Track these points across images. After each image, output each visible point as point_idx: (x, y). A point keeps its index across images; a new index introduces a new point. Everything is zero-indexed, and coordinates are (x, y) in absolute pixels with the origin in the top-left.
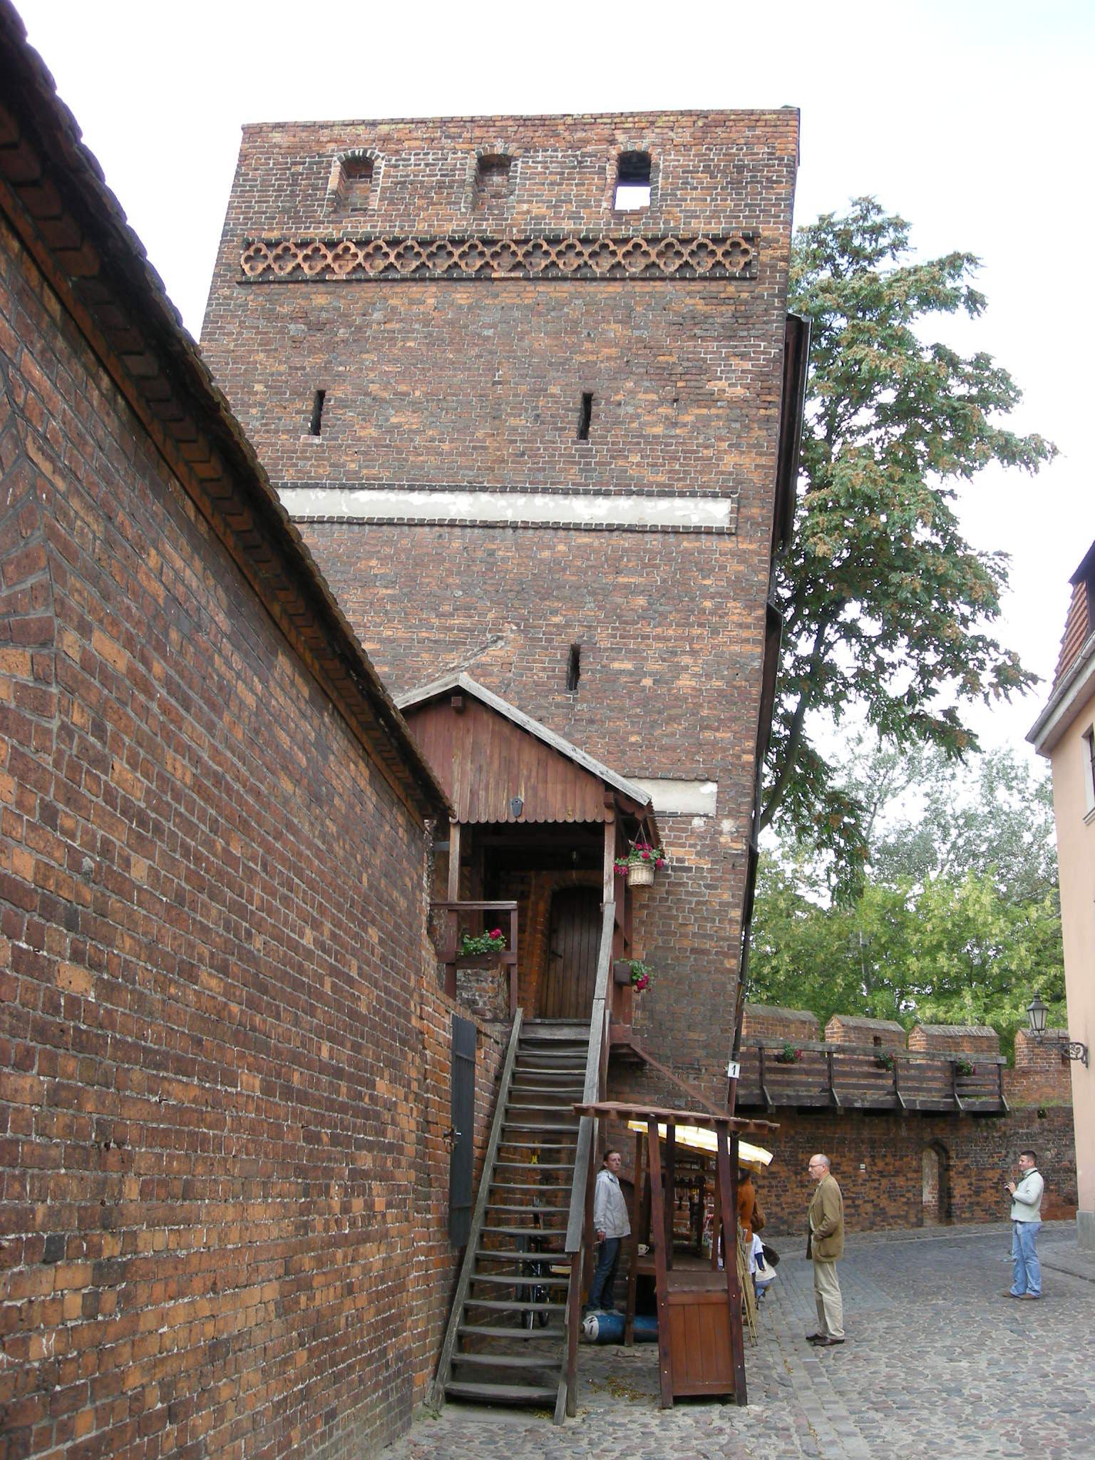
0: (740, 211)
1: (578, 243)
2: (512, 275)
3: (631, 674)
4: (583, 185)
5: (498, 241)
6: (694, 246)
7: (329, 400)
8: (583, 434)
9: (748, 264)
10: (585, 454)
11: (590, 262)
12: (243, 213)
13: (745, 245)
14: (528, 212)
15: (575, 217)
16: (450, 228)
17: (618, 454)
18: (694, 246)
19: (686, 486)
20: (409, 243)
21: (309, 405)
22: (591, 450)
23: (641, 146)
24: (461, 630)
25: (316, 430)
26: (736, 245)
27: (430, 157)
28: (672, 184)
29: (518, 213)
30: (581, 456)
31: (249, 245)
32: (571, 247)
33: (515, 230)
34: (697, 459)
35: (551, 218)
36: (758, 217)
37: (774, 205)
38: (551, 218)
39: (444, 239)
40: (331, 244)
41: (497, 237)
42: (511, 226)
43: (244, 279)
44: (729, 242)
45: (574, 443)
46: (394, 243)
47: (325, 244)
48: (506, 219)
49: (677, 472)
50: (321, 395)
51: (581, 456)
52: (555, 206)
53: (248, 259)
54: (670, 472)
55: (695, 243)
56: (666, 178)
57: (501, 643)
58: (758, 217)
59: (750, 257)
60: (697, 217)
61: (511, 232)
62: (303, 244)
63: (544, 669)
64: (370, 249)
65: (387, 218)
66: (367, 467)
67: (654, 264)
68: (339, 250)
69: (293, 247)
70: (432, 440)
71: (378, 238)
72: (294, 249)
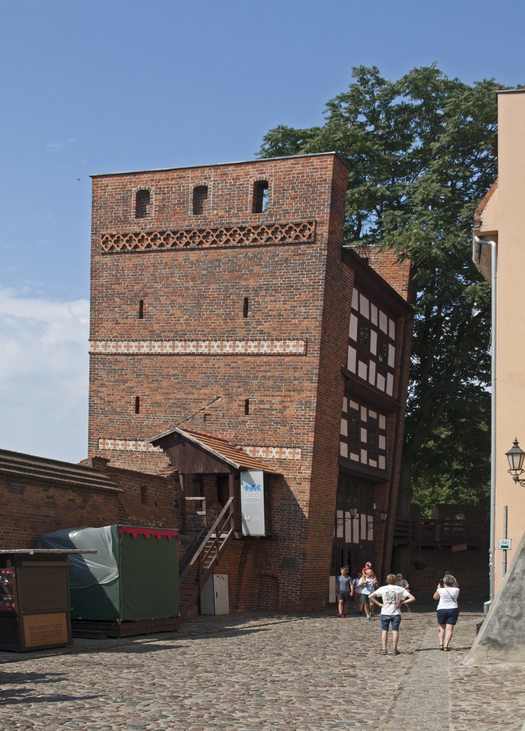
0: (308, 209)
1: (238, 230)
2: (213, 246)
3: (268, 409)
4: (239, 199)
5: (204, 230)
6: (287, 228)
7: (145, 304)
8: (246, 315)
9: (310, 235)
10: (247, 324)
11: (244, 238)
12: (98, 220)
13: (309, 226)
14: (217, 214)
15: (236, 215)
16: (185, 225)
17: (259, 323)
18: (287, 228)
19: (287, 336)
20: (168, 232)
21: (138, 307)
22: (249, 322)
23: (264, 177)
24: (205, 395)
25: (141, 316)
26: (305, 226)
27: (174, 189)
28: (277, 197)
29: (213, 216)
30: (245, 325)
31: (103, 236)
32: (236, 231)
33: (212, 224)
34: (291, 324)
35: (227, 217)
36: (315, 211)
37: (322, 205)
38: (227, 217)
39: (182, 230)
40: (137, 235)
41: (203, 228)
42: (210, 222)
43: (103, 252)
44: (302, 225)
45: (242, 319)
46: (162, 233)
47: (134, 234)
48: (208, 219)
49: (283, 330)
50: (142, 302)
51: (245, 325)
52: (229, 211)
53: (104, 243)
54: (280, 330)
55: (287, 227)
56: (275, 194)
57: (220, 399)
58: (315, 211)
59: (311, 232)
60: (289, 213)
61: (210, 225)
62: (125, 235)
63: (236, 409)
64: (152, 236)
65: (158, 220)
66: (163, 332)
67: (270, 238)
68: (140, 237)
69: (121, 236)
70: (187, 320)
71: (156, 231)
72: (122, 238)
